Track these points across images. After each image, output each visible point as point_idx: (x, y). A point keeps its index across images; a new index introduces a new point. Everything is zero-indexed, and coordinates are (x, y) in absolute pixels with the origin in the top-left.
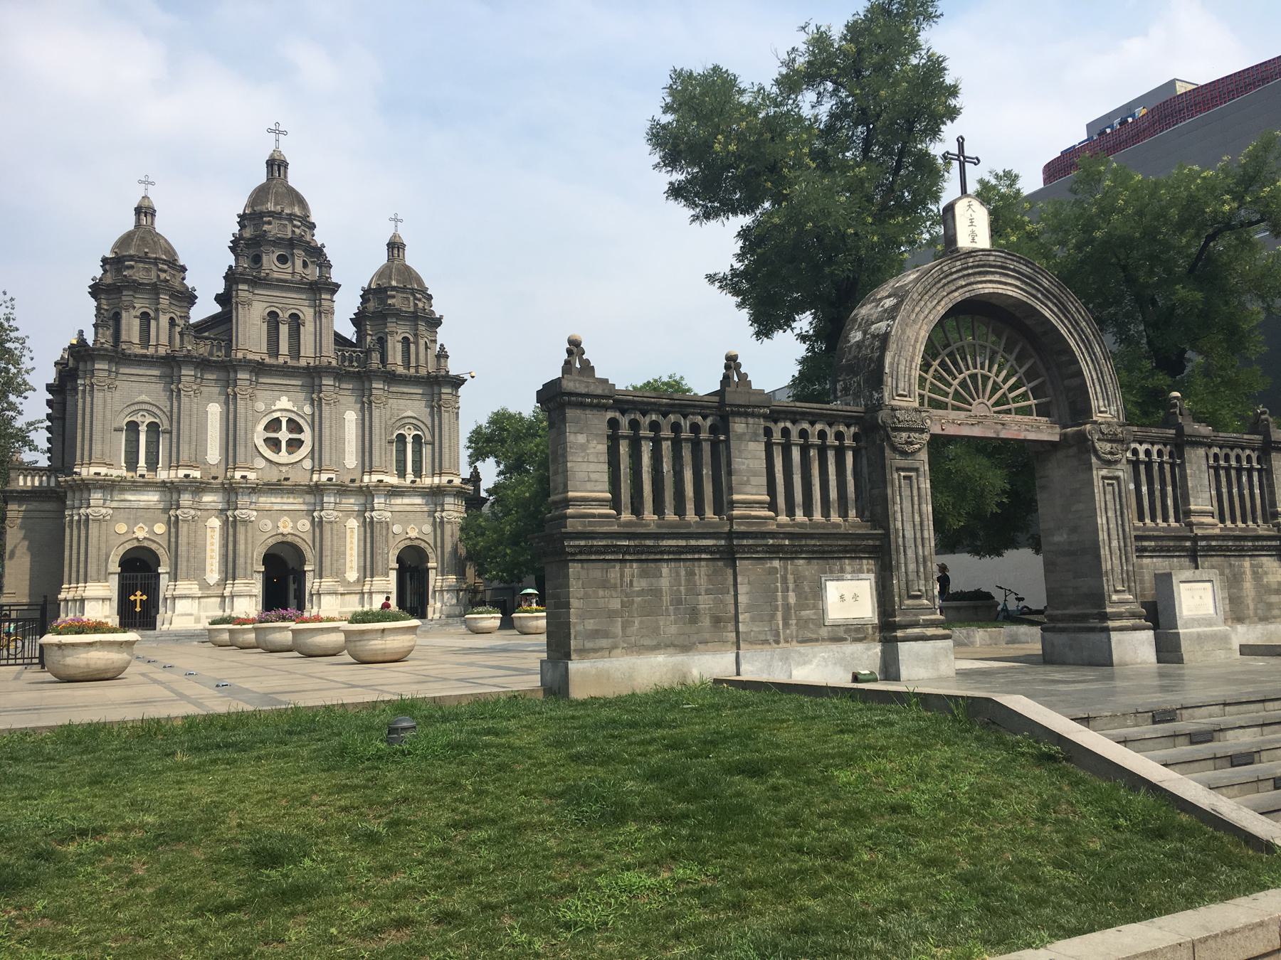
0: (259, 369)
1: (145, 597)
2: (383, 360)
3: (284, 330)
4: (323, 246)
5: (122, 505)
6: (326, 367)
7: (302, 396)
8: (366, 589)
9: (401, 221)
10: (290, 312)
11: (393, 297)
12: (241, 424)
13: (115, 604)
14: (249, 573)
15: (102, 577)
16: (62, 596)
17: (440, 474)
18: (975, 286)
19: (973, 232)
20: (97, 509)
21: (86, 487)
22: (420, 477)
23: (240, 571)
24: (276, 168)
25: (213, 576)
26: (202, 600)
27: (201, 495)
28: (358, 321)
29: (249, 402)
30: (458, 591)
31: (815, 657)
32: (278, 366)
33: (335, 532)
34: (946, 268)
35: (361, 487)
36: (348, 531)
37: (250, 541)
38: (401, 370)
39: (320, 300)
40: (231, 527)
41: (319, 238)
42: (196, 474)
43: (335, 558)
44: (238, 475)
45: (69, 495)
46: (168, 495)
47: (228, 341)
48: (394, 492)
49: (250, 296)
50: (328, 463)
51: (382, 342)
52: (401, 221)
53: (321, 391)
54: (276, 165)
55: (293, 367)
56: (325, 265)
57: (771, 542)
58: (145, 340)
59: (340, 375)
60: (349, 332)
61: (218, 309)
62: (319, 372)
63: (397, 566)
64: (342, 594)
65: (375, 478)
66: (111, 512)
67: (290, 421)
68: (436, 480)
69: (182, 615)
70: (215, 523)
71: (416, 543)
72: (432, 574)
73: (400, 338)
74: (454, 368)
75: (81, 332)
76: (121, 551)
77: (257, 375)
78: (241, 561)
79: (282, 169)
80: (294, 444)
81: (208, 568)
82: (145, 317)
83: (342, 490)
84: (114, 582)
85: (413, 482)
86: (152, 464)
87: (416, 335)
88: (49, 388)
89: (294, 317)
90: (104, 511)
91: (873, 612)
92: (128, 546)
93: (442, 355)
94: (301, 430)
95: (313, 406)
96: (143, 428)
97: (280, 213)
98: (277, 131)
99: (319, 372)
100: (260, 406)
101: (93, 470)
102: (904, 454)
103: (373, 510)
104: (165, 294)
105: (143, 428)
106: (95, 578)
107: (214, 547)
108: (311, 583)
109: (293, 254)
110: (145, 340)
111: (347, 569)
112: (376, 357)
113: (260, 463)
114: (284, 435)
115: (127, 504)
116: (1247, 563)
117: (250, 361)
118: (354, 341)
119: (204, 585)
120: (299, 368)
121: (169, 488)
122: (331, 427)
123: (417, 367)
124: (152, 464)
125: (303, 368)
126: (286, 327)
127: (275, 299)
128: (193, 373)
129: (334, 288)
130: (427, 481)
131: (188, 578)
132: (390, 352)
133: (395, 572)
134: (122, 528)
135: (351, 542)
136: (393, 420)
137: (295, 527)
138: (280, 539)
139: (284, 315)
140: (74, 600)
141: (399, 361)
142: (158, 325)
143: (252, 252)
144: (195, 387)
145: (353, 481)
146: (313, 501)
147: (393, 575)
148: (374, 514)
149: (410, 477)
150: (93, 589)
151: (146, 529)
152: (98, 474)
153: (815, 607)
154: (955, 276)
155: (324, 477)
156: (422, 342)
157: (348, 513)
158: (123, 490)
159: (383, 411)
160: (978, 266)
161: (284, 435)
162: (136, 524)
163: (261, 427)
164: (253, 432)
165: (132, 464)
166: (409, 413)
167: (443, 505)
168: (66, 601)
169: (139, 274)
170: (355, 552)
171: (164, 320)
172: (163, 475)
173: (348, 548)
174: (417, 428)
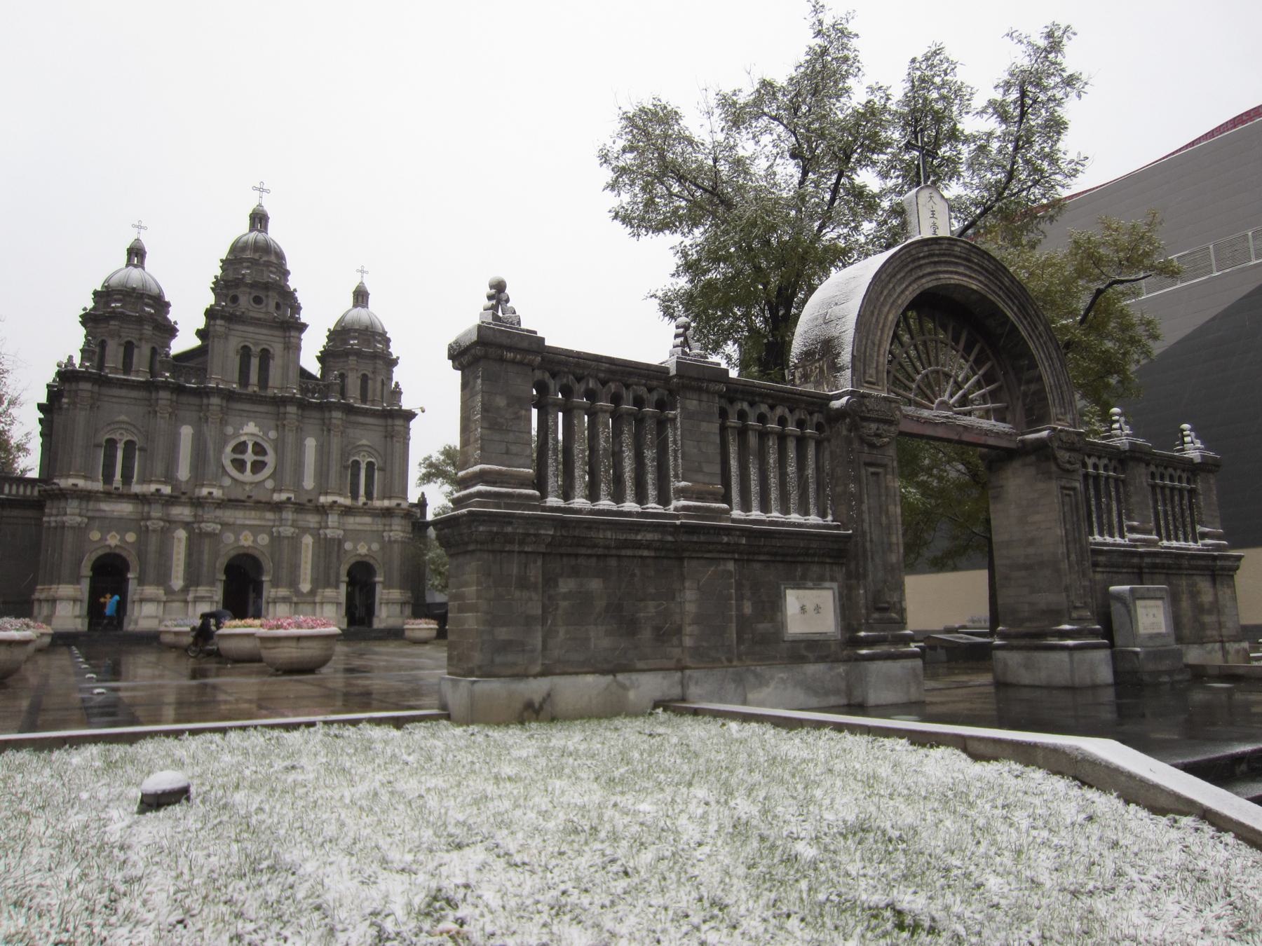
2: (343, 394)
3: (255, 362)
4: (295, 290)
5: (97, 514)
8: (318, 599)
10: (261, 347)
13: (85, 606)
16: (37, 595)
17: (390, 498)
18: (942, 276)
19: (934, 224)
20: (73, 517)
21: (63, 495)
24: (257, 220)
25: (178, 583)
27: (170, 508)
28: (323, 358)
31: (772, 678)
32: (247, 395)
34: (914, 252)
36: (303, 546)
39: (289, 337)
40: (196, 539)
41: (292, 283)
42: (167, 490)
44: (205, 491)
45: (48, 503)
46: (140, 507)
47: (202, 372)
48: (348, 511)
53: (285, 419)
54: (259, 219)
56: (297, 308)
57: (725, 539)
58: (127, 368)
59: (303, 405)
60: (314, 368)
61: (196, 342)
64: (296, 603)
65: (330, 499)
66: (86, 520)
67: (256, 444)
70: (181, 534)
71: (367, 559)
72: (379, 588)
73: (360, 375)
74: (406, 404)
75: (71, 358)
76: (94, 556)
77: (228, 401)
79: (263, 222)
80: (258, 466)
81: (174, 575)
82: (129, 348)
83: (300, 508)
84: (85, 585)
85: (365, 504)
86: (127, 478)
88: (41, 407)
90: (79, 519)
91: (836, 626)
92: (100, 552)
93: (397, 393)
94: (264, 452)
101: (71, 481)
102: (872, 446)
103: (327, 527)
108: (269, 592)
109: (267, 296)
110: (127, 368)
113: (227, 482)
114: (249, 457)
115: (103, 514)
116: (1184, 582)
118: (319, 376)
119: (170, 591)
124: (127, 478)
125: (270, 398)
128: (169, 397)
129: (303, 327)
130: (378, 503)
134: (95, 535)
135: (306, 557)
136: (350, 447)
137: (255, 541)
138: (241, 552)
139: (255, 350)
140: (47, 600)
141: (357, 394)
143: (231, 292)
144: (170, 410)
145: (310, 501)
147: (343, 588)
148: (328, 531)
149: (362, 499)
150: (66, 590)
151: (118, 537)
152: (75, 485)
153: (772, 620)
154: (922, 262)
156: (379, 379)
158: (98, 500)
160: (944, 255)
161: (249, 457)
162: (109, 532)
163: (229, 449)
164: (220, 451)
165: (108, 478)
166: (364, 442)
167: (391, 525)
168: (40, 601)
170: (309, 566)
171: (146, 350)
172: (136, 488)
173: (303, 563)
174: (370, 455)
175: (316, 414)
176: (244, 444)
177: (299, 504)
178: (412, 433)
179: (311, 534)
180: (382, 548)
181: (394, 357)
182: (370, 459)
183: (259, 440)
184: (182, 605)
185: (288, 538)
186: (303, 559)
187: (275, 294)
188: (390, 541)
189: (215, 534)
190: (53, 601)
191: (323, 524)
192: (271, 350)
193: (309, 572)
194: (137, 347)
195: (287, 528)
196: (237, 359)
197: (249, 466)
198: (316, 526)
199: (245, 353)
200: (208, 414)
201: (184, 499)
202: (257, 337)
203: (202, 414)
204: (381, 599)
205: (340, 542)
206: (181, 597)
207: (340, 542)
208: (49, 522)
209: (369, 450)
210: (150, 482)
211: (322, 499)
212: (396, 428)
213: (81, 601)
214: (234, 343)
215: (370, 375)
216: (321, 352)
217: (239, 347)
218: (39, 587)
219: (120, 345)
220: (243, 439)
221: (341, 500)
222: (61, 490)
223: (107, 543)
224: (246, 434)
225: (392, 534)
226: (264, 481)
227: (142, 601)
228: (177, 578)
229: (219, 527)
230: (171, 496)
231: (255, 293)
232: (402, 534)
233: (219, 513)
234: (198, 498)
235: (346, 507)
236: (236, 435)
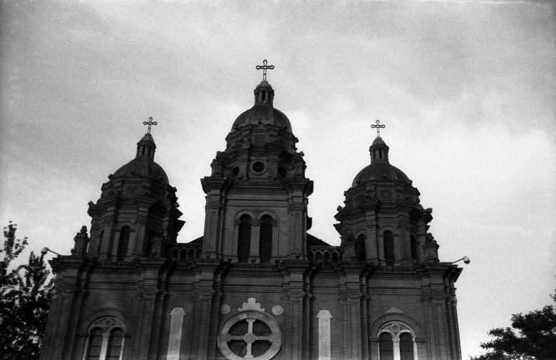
3: (255, 232)
67: (257, 322)
74: (444, 256)
94: (268, 331)
97: (257, 126)
100: (227, 309)
127: (248, 203)
163: (225, 330)
164: (218, 333)
166: (394, 310)
176: (244, 322)
182: (403, 331)
183: (261, 317)
192: (274, 216)
194: (133, 231)
197: (249, 347)
202: (261, 203)
214: (232, 215)
215: (395, 231)
216: (335, 217)
217: (238, 218)
220: (244, 316)
224: (248, 312)
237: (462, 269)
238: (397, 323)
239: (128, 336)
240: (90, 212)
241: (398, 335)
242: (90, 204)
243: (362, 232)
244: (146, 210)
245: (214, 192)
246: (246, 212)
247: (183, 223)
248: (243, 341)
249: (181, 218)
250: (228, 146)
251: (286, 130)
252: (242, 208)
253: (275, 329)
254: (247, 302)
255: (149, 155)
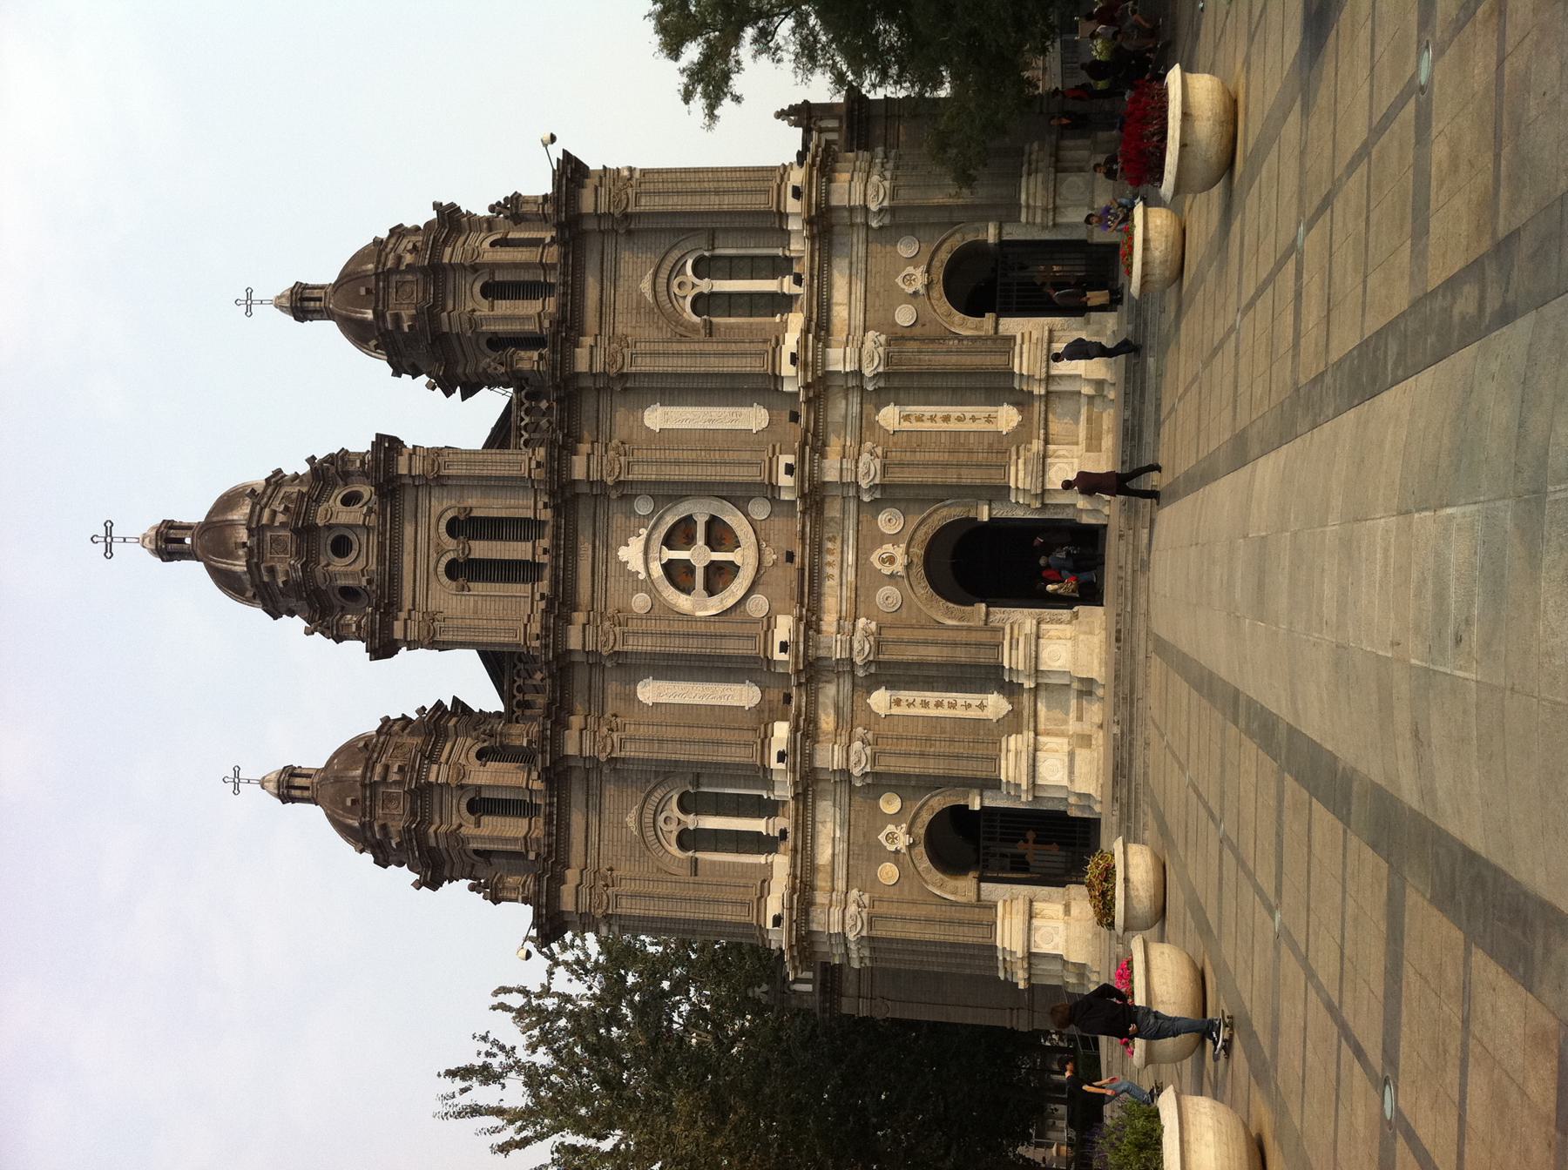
0: (561, 605)
1: (1031, 835)
3: (482, 549)
4: (311, 460)
6: (551, 471)
7: (618, 520)
8: (1039, 390)
9: (249, 292)
10: (445, 537)
11: (397, 318)
12: (675, 646)
13: (1042, 891)
14: (985, 637)
15: (985, 916)
17: (783, 216)
22: (789, 260)
23: (984, 657)
25: (995, 705)
26: (1041, 727)
29: (633, 626)
30: (1057, 171)
32: (555, 568)
33: (908, 457)
35: (808, 401)
36: (906, 426)
37: (920, 635)
38: (551, 304)
39: (413, 477)
43: (963, 457)
44: (778, 656)
46: (821, 786)
48: (819, 328)
49: (416, 615)
50: (755, 470)
51: (498, 342)
52: (249, 292)
53: (602, 482)
55: (556, 537)
60: (491, 403)
62: (562, 487)
63: (989, 318)
64: (1047, 442)
65: (787, 369)
66: (854, 893)
67: (668, 542)
68: (794, 225)
69: (1071, 772)
70: (880, 700)
72: (1014, 233)
73: (485, 303)
74: (539, 184)
78: (962, 656)
79: (173, 533)
80: (719, 535)
82: (481, 805)
84: (994, 891)
85: (798, 280)
87: (475, 268)
89: (454, 528)
92: (924, 863)
93: (513, 208)
94: (687, 523)
95: (636, 496)
96: (691, 821)
97: (250, 550)
98: (108, 540)
99: (562, 487)
100: (640, 602)
103: (859, 374)
104: (428, 772)
105: (691, 821)
106: (986, 931)
107: (932, 702)
108: (1018, 509)
109: (329, 527)
111: (991, 427)
112: (528, 360)
113: (758, 605)
114: (699, 555)
115: (841, 860)
117: (545, 627)
119: (1013, 724)
120: (557, 527)
121: (808, 783)
122: (677, 463)
123: (544, 266)
126: (472, 543)
129: (387, 446)
130: (798, 246)
131: (995, 760)
132: (516, 327)
133: (1003, 321)
137: (894, 539)
138: (919, 570)
139: (451, 548)
141: (531, 307)
142: (489, 787)
143: (337, 600)
145: (795, 417)
146: (837, 504)
147: (1012, 325)
148: (868, 371)
149: (787, 285)
150: (1009, 936)
151: (890, 828)
155: (785, 480)
156: (491, 256)
157: (865, 427)
159: (641, 347)
161: (699, 555)
163: (683, 602)
166: (646, 286)
167: (851, 209)
169: (396, 818)
170: (955, 411)
172: (783, 791)
175: (588, 406)
176: (668, 567)
177: (804, 444)
178: (617, 160)
179: (878, 411)
180: (911, 229)
181: (433, 215)
184: (1042, 694)
185: (884, 467)
186: (940, 426)
187: (321, 510)
188: (892, 210)
189: (880, 628)
190: (1031, 956)
191: (852, 383)
192: (450, 514)
193: (969, 410)
195: (862, 469)
196: (478, 588)
198: (855, 399)
199: (463, 571)
200: (605, 651)
201: (798, 698)
202: (422, 544)
203: (609, 665)
204: (1044, 227)
205: (897, 338)
206: (1026, 699)
207: (897, 338)
208: (861, 959)
209: (664, 275)
210: (767, 770)
211: (788, 387)
212: (603, 209)
213: (1031, 902)
214: (446, 598)
216: (448, 395)
218: (1001, 975)
219: (478, 824)
220: (657, 570)
221: (791, 342)
222: (791, 947)
223: (904, 851)
225: (874, 207)
226: (752, 523)
227: (1034, 785)
228: (982, 706)
229: (862, 622)
230: (795, 729)
231: (326, 556)
232: (875, 178)
233: (829, 622)
234: (798, 672)
235: (806, 331)
236: (649, 586)
237: (564, 151)
238: (675, 282)
239: (697, 780)
240: (434, 885)
241: (697, 281)
242: (418, 885)
243: (484, 346)
244: (435, 767)
245: (398, 634)
246: (442, 568)
247: (456, 700)
248: (707, 568)
249: (448, 703)
250: (292, 614)
251: (259, 490)
252: (432, 577)
253: (682, 510)
254: (628, 562)
255: (308, 776)
